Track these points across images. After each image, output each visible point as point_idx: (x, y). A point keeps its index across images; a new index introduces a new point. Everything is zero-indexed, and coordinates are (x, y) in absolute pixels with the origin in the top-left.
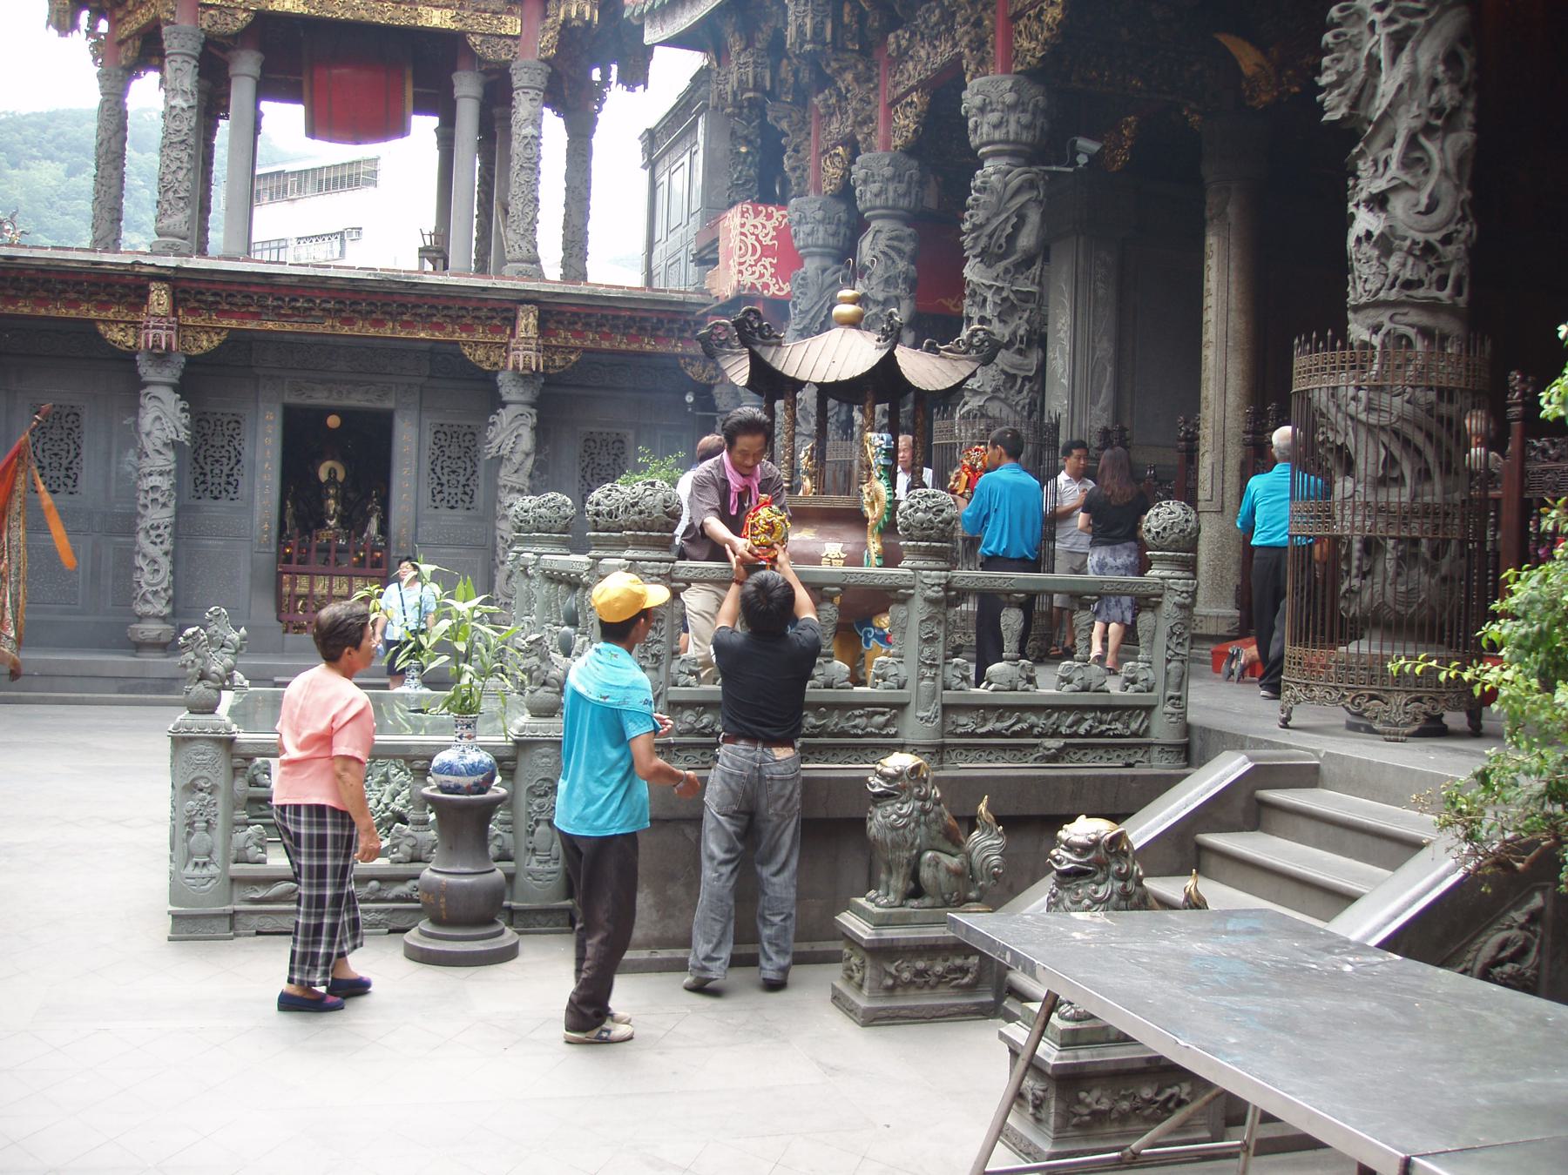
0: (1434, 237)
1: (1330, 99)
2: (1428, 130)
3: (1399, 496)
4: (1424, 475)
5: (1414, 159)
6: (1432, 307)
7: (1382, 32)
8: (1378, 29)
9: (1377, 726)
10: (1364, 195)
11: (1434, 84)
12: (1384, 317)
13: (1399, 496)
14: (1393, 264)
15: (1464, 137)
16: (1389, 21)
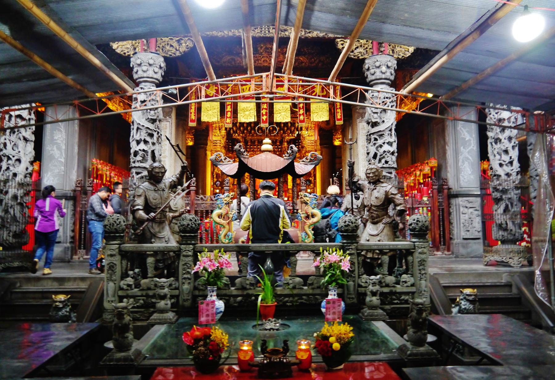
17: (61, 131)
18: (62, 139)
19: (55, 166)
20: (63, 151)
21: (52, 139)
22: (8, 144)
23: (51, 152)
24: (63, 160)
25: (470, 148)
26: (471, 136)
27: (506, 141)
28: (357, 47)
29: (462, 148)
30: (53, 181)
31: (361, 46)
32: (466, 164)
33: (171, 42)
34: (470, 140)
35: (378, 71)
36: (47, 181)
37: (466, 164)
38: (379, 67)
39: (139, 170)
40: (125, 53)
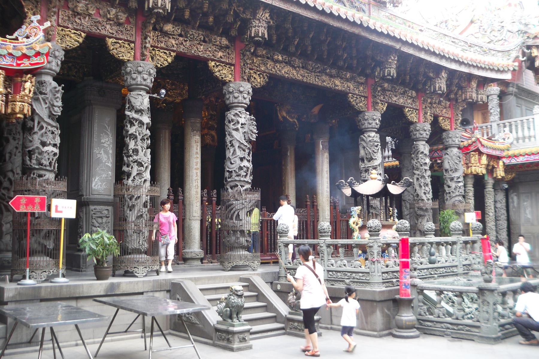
17: (108, 134)
18: (109, 143)
19: (103, 170)
20: (110, 156)
21: (100, 143)
22: (140, 151)
23: (99, 156)
24: (110, 165)
30: (101, 186)
33: (254, 76)
35: (374, 122)
36: (95, 186)
38: (375, 120)
39: (243, 184)
40: (222, 78)
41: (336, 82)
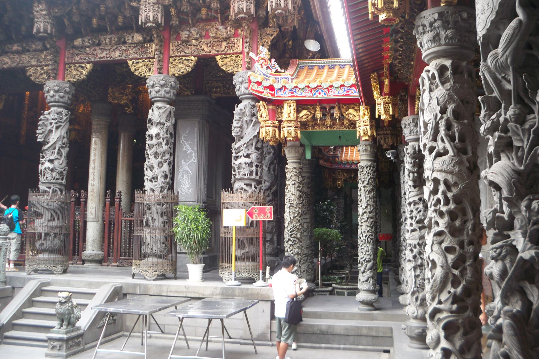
0: (62, 170)
1: (40, 136)
2: (62, 147)
3: (53, 224)
4: (58, 219)
5: (59, 153)
6: (61, 184)
7: (55, 126)
8: (53, 124)
9: (55, 272)
10: (48, 159)
11: (64, 137)
12: (52, 186)
13: (53, 224)
14: (54, 174)
15: (67, 149)
16: (56, 123)
25: (190, 161)
26: (193, 149)
27: (152, 157)
28: (42, 74)
29: (183, 161)
31: (44, 73)
32: (186, 177)
34: (191, 153)
37: (186, 177)
41: (5, 59)
